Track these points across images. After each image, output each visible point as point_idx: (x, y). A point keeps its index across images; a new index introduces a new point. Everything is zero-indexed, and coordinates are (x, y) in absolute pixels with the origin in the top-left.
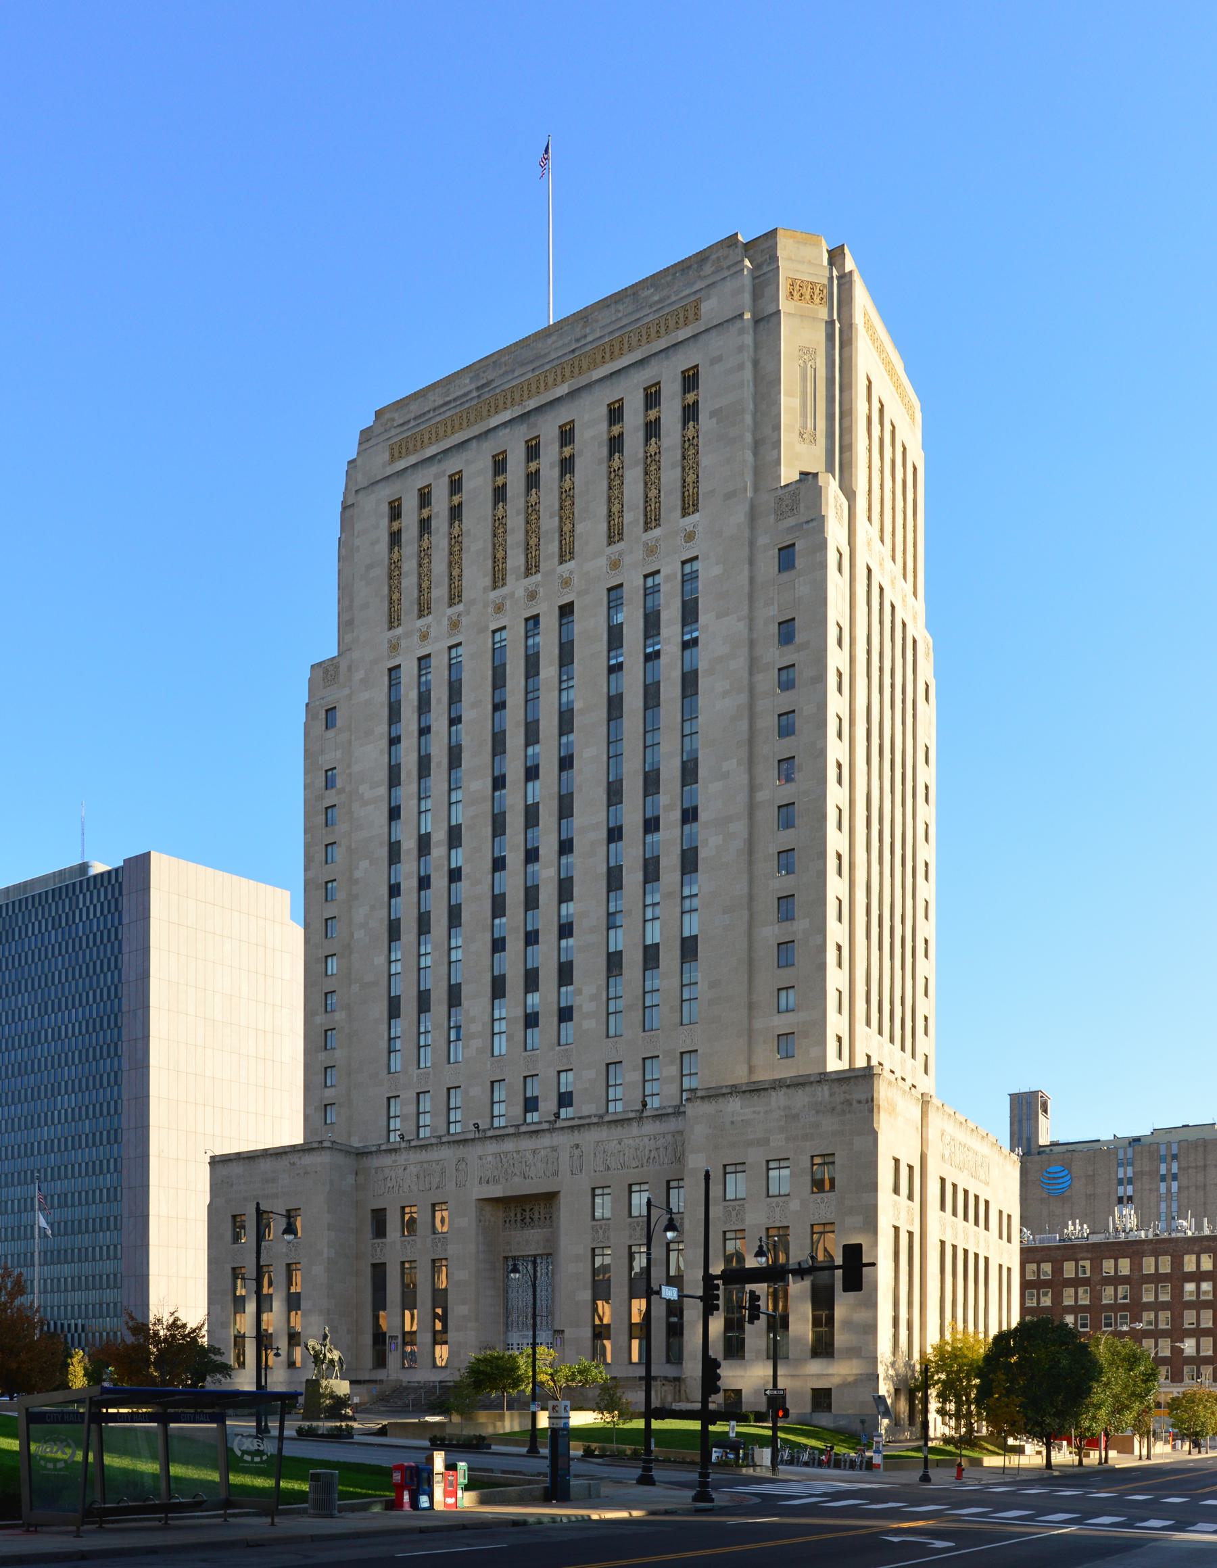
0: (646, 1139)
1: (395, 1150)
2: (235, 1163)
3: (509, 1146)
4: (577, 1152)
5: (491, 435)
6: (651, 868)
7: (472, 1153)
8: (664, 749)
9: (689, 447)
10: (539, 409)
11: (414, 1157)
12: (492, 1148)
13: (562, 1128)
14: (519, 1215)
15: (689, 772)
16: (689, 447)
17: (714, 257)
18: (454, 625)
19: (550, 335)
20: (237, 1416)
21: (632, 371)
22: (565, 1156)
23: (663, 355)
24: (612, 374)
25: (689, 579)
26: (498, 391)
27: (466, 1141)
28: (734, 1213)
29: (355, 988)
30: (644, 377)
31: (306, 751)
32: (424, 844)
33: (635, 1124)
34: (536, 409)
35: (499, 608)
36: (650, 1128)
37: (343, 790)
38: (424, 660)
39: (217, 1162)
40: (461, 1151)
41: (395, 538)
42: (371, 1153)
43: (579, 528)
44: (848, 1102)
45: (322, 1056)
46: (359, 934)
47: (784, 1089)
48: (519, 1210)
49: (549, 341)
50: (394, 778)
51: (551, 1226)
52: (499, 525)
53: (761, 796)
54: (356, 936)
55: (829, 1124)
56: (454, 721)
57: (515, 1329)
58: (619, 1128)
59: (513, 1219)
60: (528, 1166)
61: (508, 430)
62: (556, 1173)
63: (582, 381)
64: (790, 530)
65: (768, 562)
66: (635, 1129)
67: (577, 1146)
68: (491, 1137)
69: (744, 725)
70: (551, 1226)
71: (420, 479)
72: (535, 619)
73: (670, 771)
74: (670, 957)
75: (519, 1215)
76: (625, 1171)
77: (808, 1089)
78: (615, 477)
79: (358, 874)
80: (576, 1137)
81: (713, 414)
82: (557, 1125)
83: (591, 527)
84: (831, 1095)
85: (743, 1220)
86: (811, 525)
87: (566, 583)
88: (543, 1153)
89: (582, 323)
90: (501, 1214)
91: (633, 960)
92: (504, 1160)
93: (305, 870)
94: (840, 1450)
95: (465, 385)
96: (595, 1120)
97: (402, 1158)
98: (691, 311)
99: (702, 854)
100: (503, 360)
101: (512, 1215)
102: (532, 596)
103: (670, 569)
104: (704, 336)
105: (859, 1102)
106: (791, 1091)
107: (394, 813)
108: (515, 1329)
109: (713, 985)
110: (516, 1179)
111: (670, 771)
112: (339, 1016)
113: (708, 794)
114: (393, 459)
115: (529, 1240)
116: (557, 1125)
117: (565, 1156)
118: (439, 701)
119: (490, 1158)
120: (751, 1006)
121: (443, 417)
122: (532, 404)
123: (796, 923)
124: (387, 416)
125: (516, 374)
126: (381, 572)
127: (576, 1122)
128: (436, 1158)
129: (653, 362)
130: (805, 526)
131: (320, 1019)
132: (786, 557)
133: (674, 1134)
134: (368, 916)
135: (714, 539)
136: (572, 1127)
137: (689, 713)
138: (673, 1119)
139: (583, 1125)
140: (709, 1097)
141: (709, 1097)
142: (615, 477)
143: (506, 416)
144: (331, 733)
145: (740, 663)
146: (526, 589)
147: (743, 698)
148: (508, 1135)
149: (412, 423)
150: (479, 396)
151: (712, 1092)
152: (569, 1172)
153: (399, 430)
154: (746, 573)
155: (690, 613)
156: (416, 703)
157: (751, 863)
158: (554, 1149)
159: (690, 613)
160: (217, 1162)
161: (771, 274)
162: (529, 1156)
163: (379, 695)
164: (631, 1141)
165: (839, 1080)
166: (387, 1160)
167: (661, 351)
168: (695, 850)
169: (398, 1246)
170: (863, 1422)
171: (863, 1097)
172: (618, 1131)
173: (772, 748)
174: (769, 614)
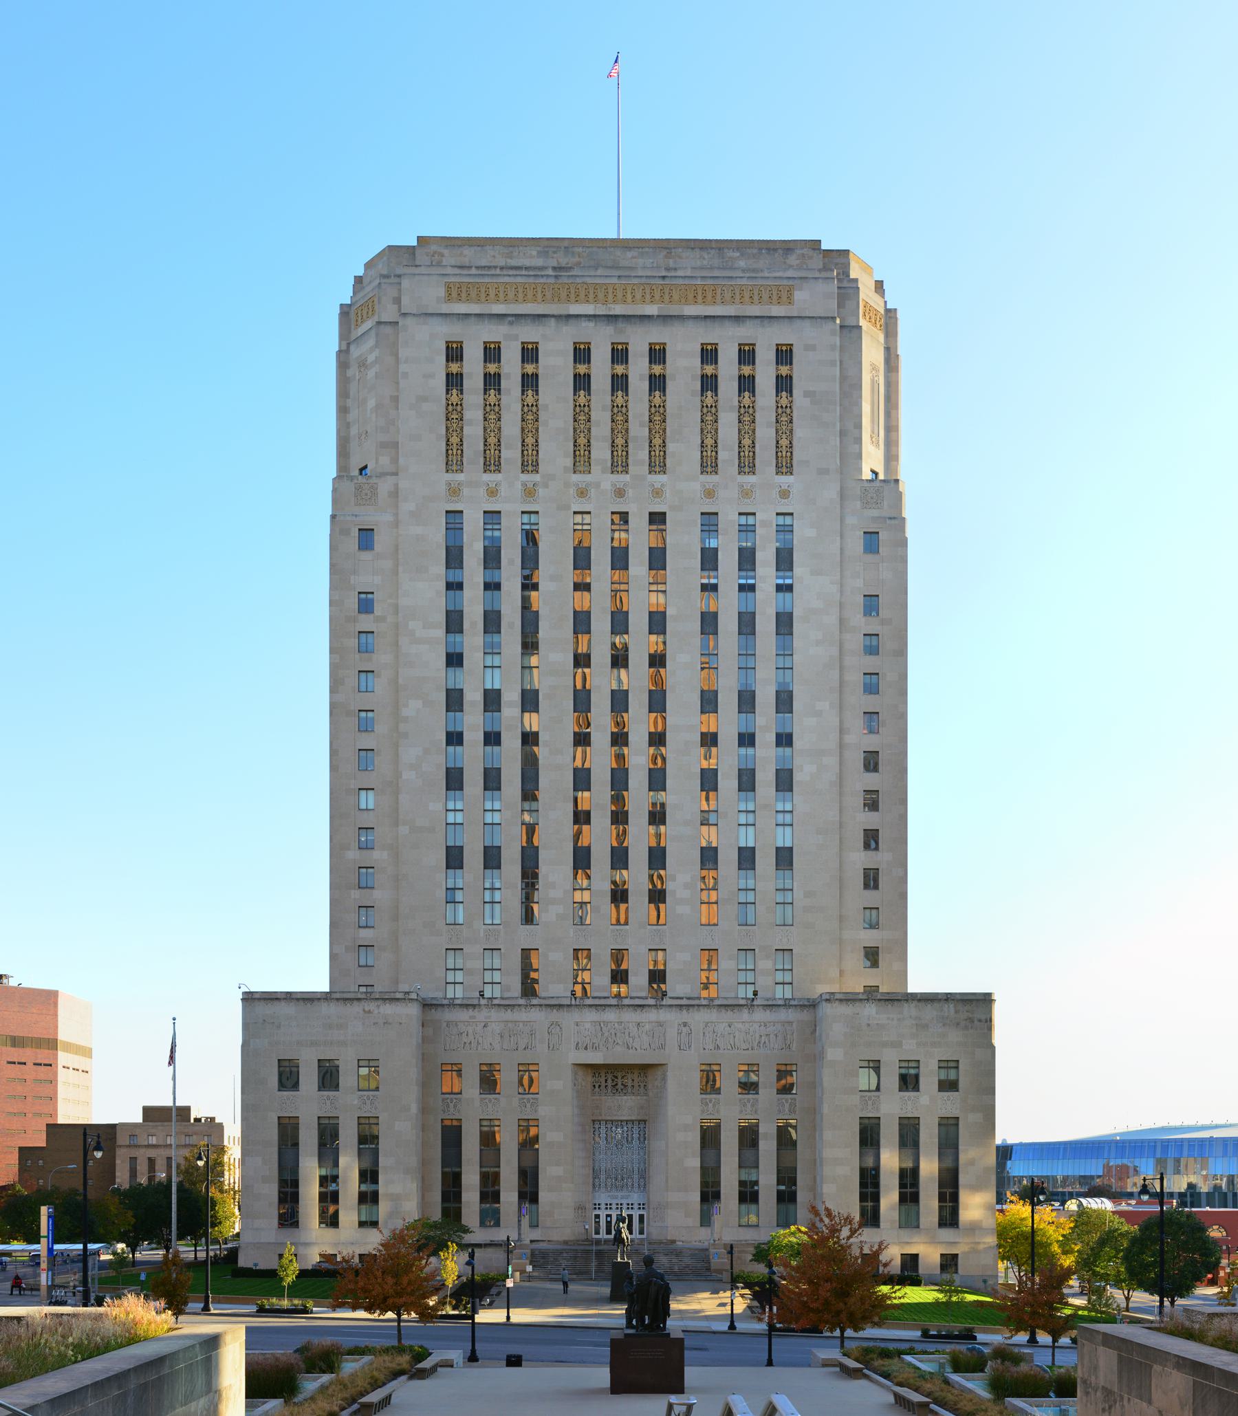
0: (756, 1026)
1: (474, 1006)
2: (283, 1003)
3: (610, 1016)
4: (685, 1030)
5: (572, 321)
6: (745, 778)
7: (568, 1019)
8: (760, 674)
9: (784, 416)
10: (627, 318)
11: (494, 1015)
12: (591, 1016)
13: (671, 1006)
14: (609, 1081)
15: (784, 701)
16: (784, 416)
17: (799, 252)
18: (529, 492)
19: (630, 249)
20: (985, 1331)
21: (727, 323)
22: (672, 1033)
23: (758, 321)
24: (706, 317)
25: (785, 530)
26: (578, 280)
27: (560, 1006)
28: (870, 1103)
29: (404, 830)
30: (745, 333)
31: (332, 566)
32: (492, 700)
33: (746, 1011)
34: (624, 316)
35: (582, 493)
36: (760, 1015)
37: (381, 619)
38: (492, 516)
39: (249, 999)
40: (555, 1015)
41: (454, 381)
42: (443, 1005)
43: (671, 447)
44: (971, 1020)
45: (356, 894)
46: (408, 775)
47: (915, 1003)
48: (610, 1077)
49: (629, 254)
50: (454, 622)
51: (646, 1094)
52: (581, 415)
53: (848, 739)
54: (404, 777)
55: (954, 1036)
56: (529, 585)
57: (603, 1190)
58: (730, 1013)
59: (603, 1084)
60: (631, 1035)
61: (591, 324)
62: (662, 1047)
63: (674, 310)
64: (875, 519)
65: (856, 543)
66: (745, 1015)
67: (685, 1024)
68: (590, 1006)
69: (835, 674)
70: (646, 1094)
71: (493, 332)
72: (624, 517)
73: (766, 697)
74: (765, 861)
75: (609, 1081)
76: (735, 1051)
77: (936, 1005)
78: (709, 416)
79: (405, 712)
80: (685, 1016)
81: (807, 394)
82: (664, 1003)
83: (684, 448)
84: (956, 1012)
85: (878, 1110)
86: (893, 522)
87: (657, 493)
88: (647, 1027)
89: (664, 252)
90: (590, 1079)
91: (727, 859)
92: (604, 1029)
93: (331, 692)
94: (1086, 1313)
95: (531, 257)
96: (704, 1002)
97: (481, 1015)
98: (784, 294)
99: (797, 777)
100: (576, 250)
101: (603, 1080)
102: (620, 493)
103: (766, 518)
104: (799, 322)
105: (980, 1021)
106: (921, 1004)
107: (454, 660)
108: (603, 1190)
109: (808, 894)
110: (618, 1049)
111: (766, 697)
112: (378, 856)
113: (803, 725)
114: (449, 298)
115: (625, 1105)
116: (664, 1003)
117: (672, 1033)
118: (511, 562)
119: (588, 1026)
120: (841, 918)
121: (507, 279)
122: (618, 309)
123: (879, 854)
124: (434, 248)
125: (599, 272)
126: (438, 408)
127: (684, 1002)
128: (524, 1019)
129: (749, 323)
130: (888, 522)
131: (353, 854)
132: (871, 540)
133: (783, 1023)
134: (423, 757)
135: (808, 501)
136: (681, 1006)
137: (785, 652)
138: (783, 1010)
139: (693, 1006)
140: (847, 1000)
141: (847, 1000)
142: (709, 416)
143: (589, 309)
144: (366, 556)
145: (832, 619)
146: (613, 485)
147: (835, 651)
148: (610, 1006)
149: (474, 271)
150: (556, 277)
151: (851, 997)
152: (677, 1047)
153: (457, 271)
154: (838, 544)
155: (785, 560)
156: (482, 556)
157: (841, 794)
158: (660, 1024)
159: (785, 560)
160: (249, 999)
161: (851, 291)
162: (634, 1030)
163: (437, 536)
164: (740, 1025)
165: (962, 1000)
166: (464, 1015)
167: (757, 317)
168: (790, 772)
169: (477, 1103)
170: (985, 1281)
171: (983, 1017)
172: (728, 1015)
173: (859, 701)
174: (858, 585)
